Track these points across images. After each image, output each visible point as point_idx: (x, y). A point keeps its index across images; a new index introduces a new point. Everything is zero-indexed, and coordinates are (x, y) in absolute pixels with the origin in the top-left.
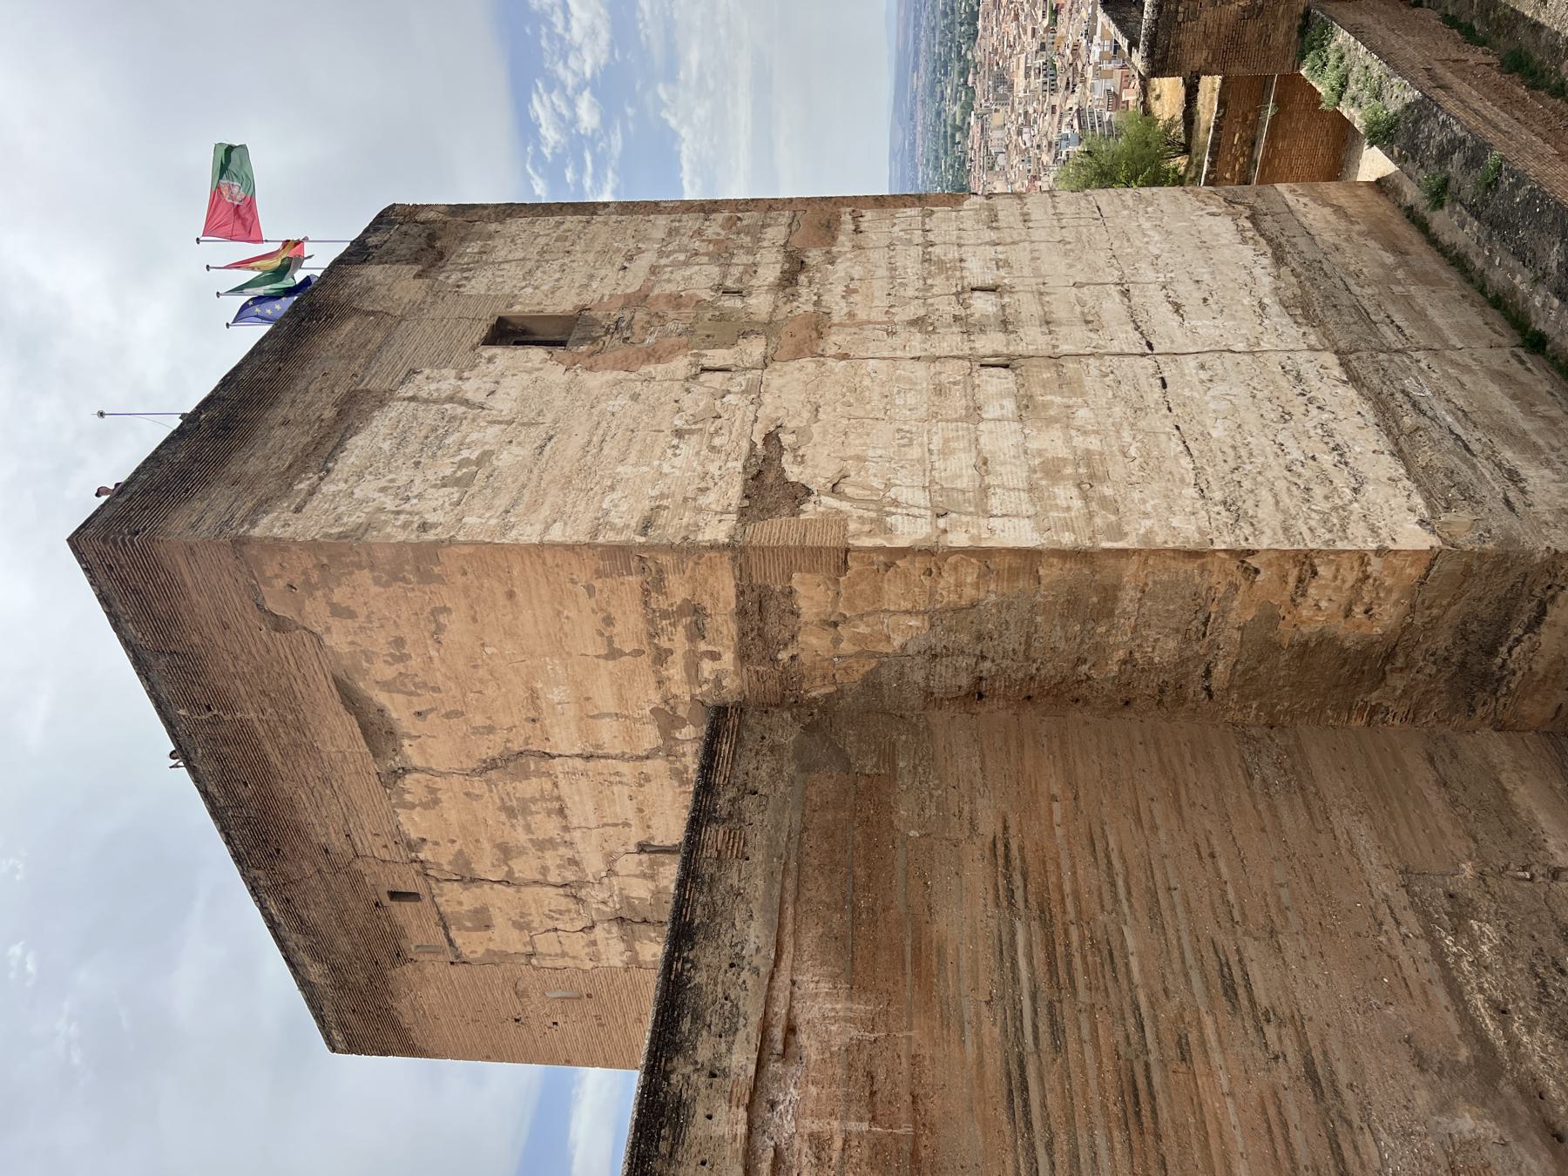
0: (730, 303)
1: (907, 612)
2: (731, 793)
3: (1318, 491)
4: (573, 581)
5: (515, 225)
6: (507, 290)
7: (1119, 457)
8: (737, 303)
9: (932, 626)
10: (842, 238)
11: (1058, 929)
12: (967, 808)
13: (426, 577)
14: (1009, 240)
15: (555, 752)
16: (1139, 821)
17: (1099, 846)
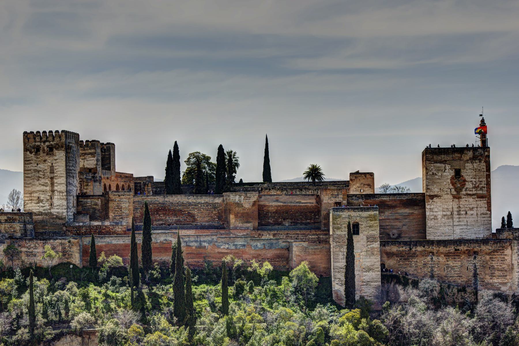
5: (483, 165)
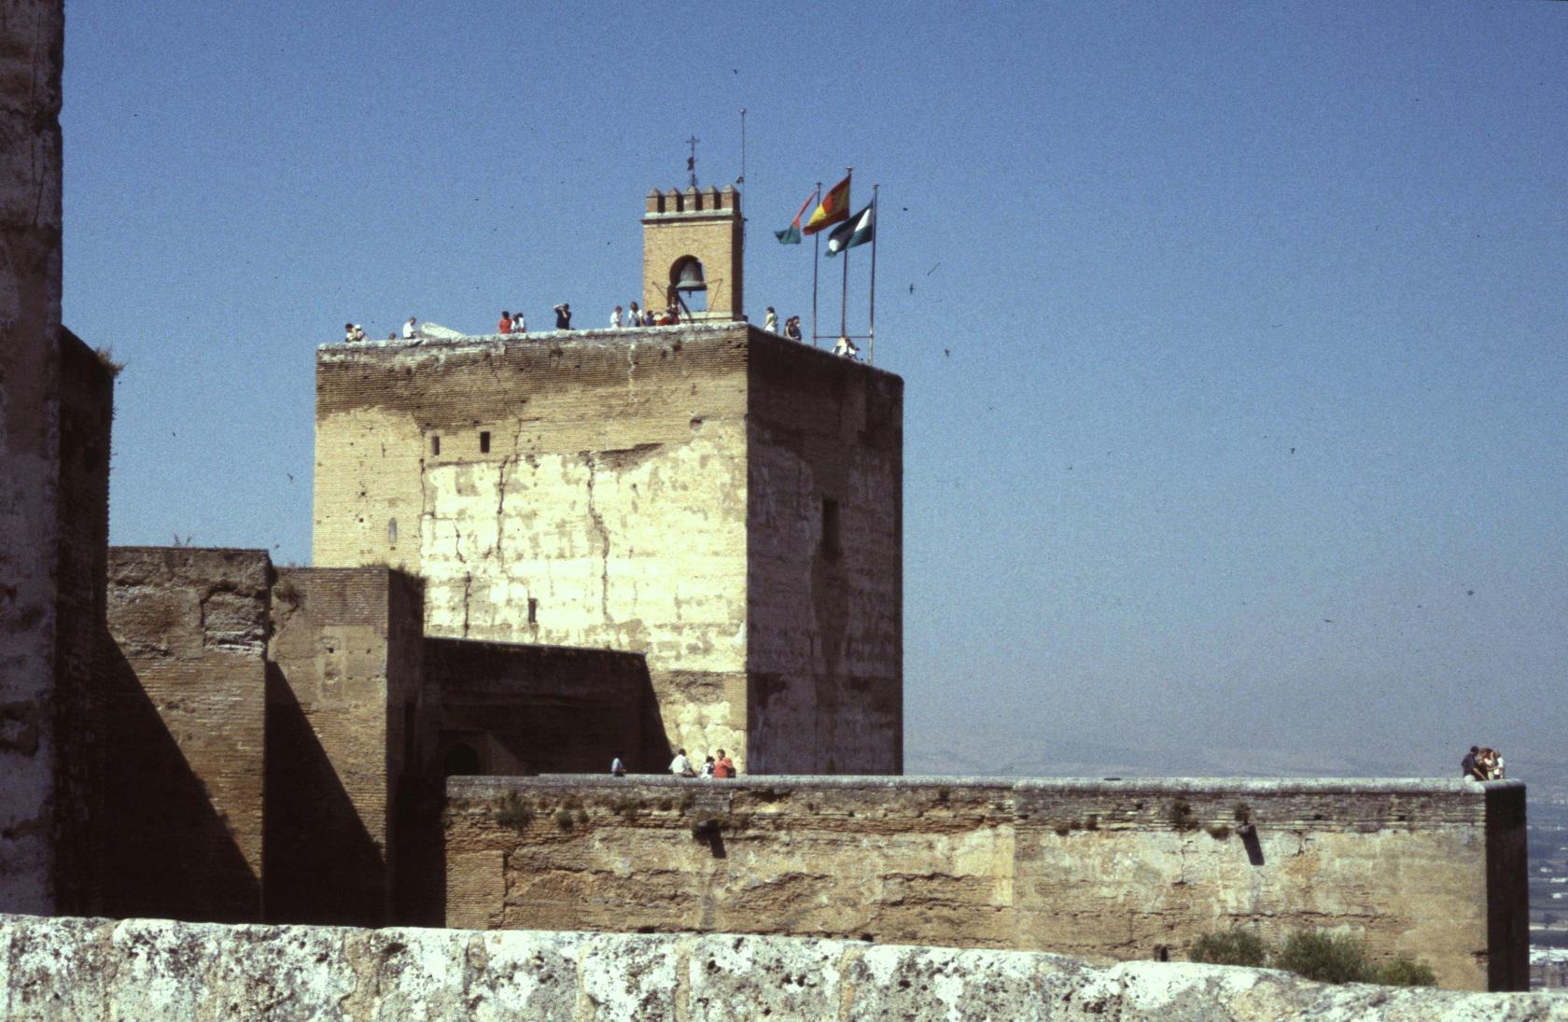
0: (844, 646)
13: (727, 512)
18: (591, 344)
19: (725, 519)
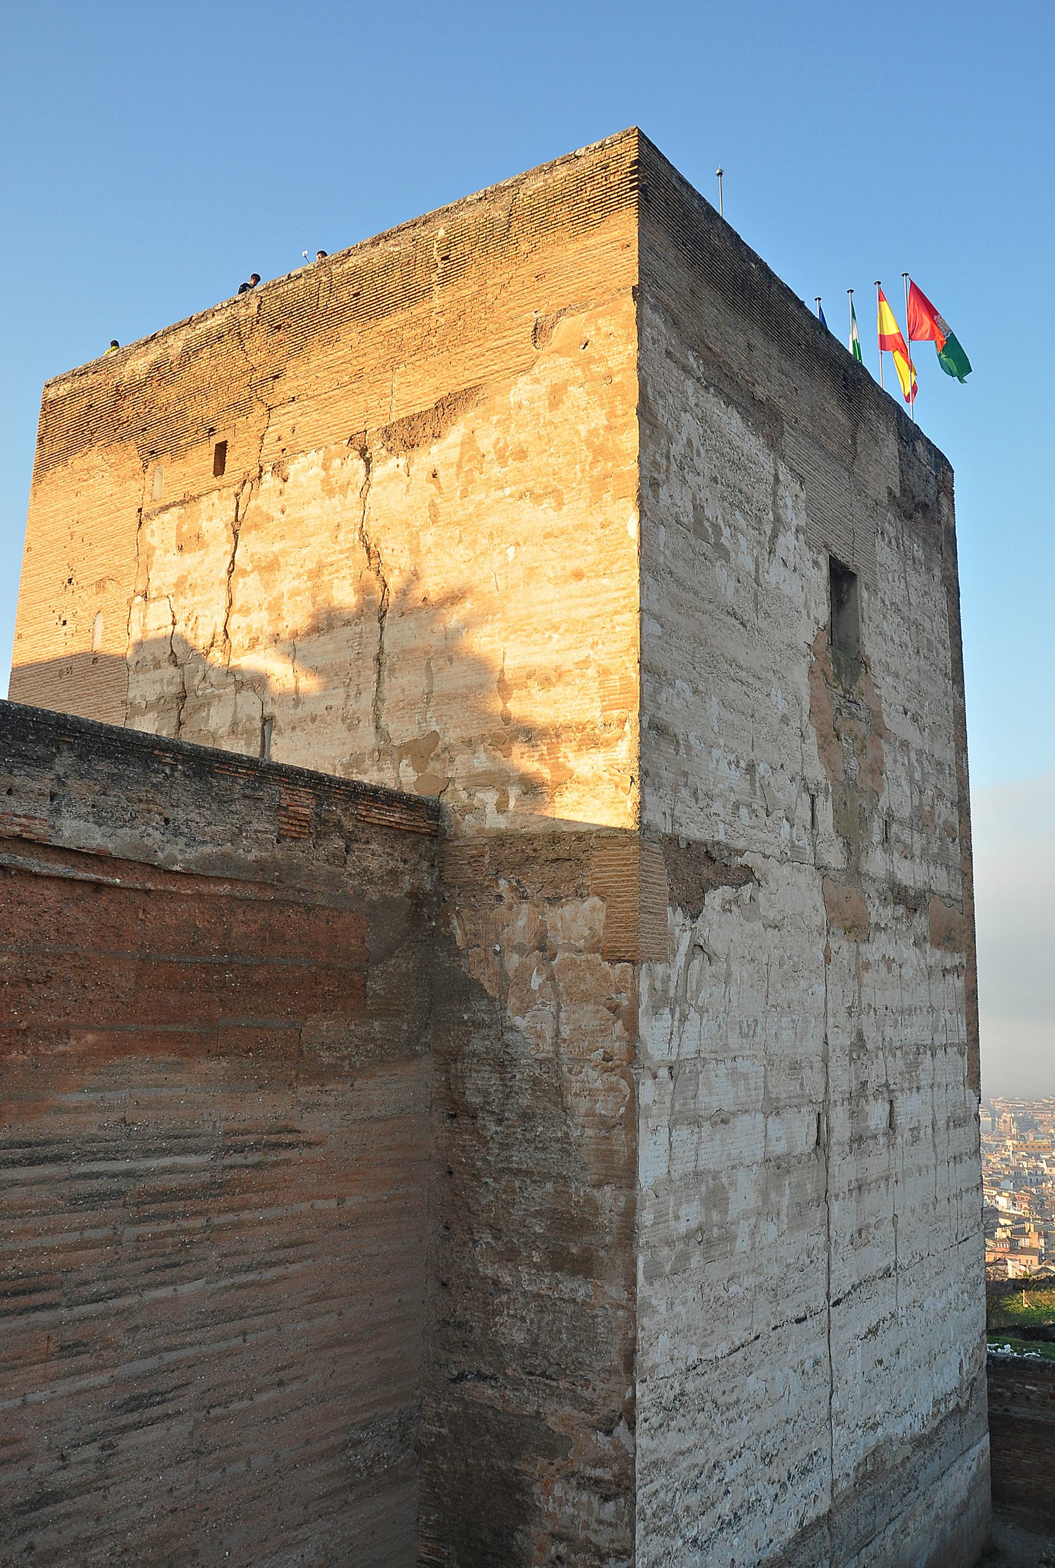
1: (557, 1033)
2: (348, 825)
3: (693, 1499)
4: (594, 644)
6: (882, 585)
7: (728, 1274)
8: (877, 838)
9: (541, 1062)
10: (938, 954)
11: (201, 1205)
12: (331, 1100)
13: (599, 485)
14: (937, 1140)
15: (386, 623)
16: (318, 1299)
17: (291, 1252)
18: (376, 254)
19: (596, 501)
